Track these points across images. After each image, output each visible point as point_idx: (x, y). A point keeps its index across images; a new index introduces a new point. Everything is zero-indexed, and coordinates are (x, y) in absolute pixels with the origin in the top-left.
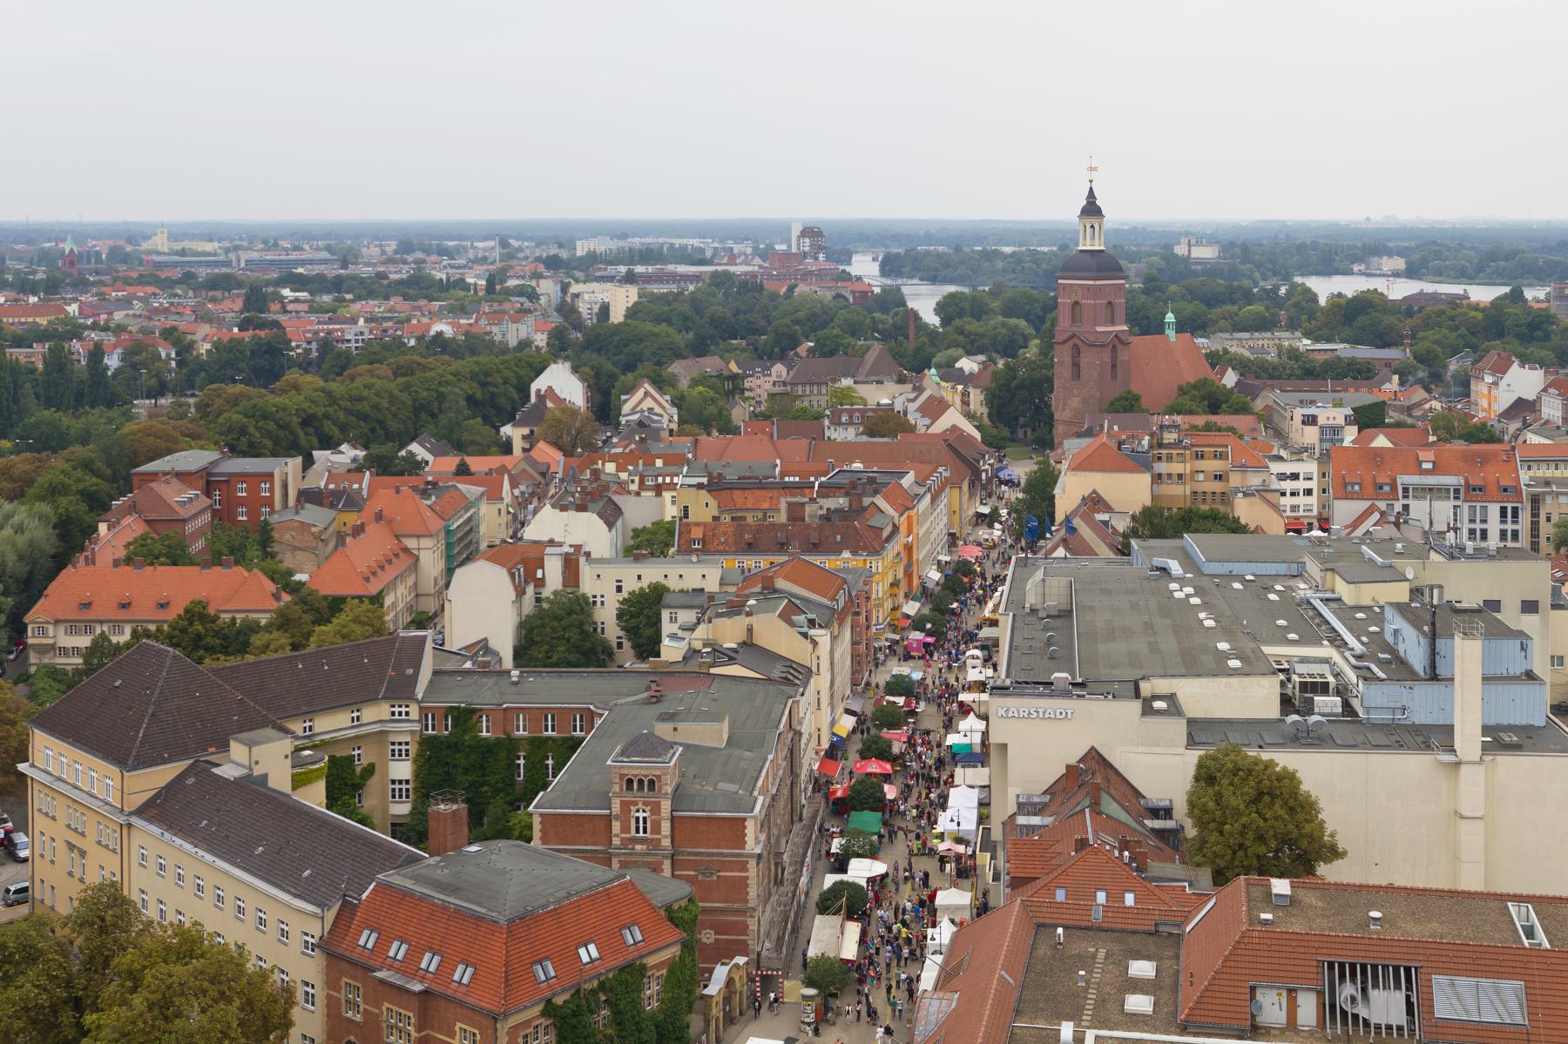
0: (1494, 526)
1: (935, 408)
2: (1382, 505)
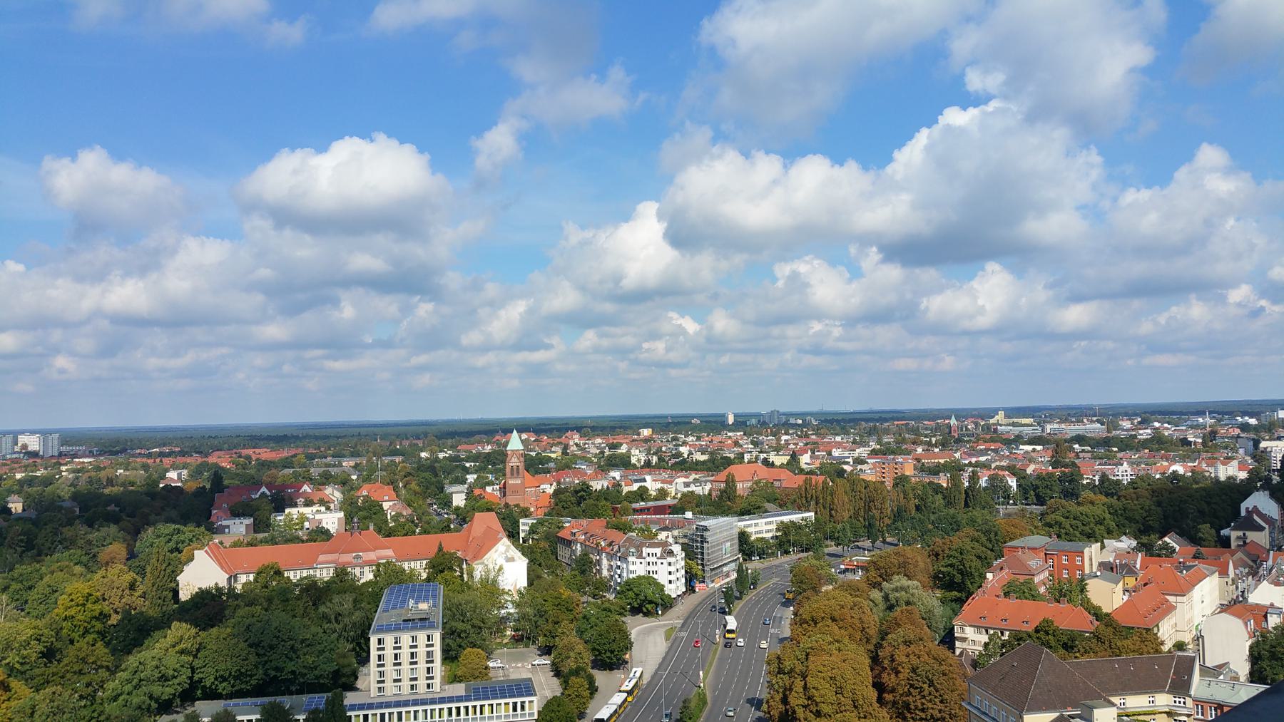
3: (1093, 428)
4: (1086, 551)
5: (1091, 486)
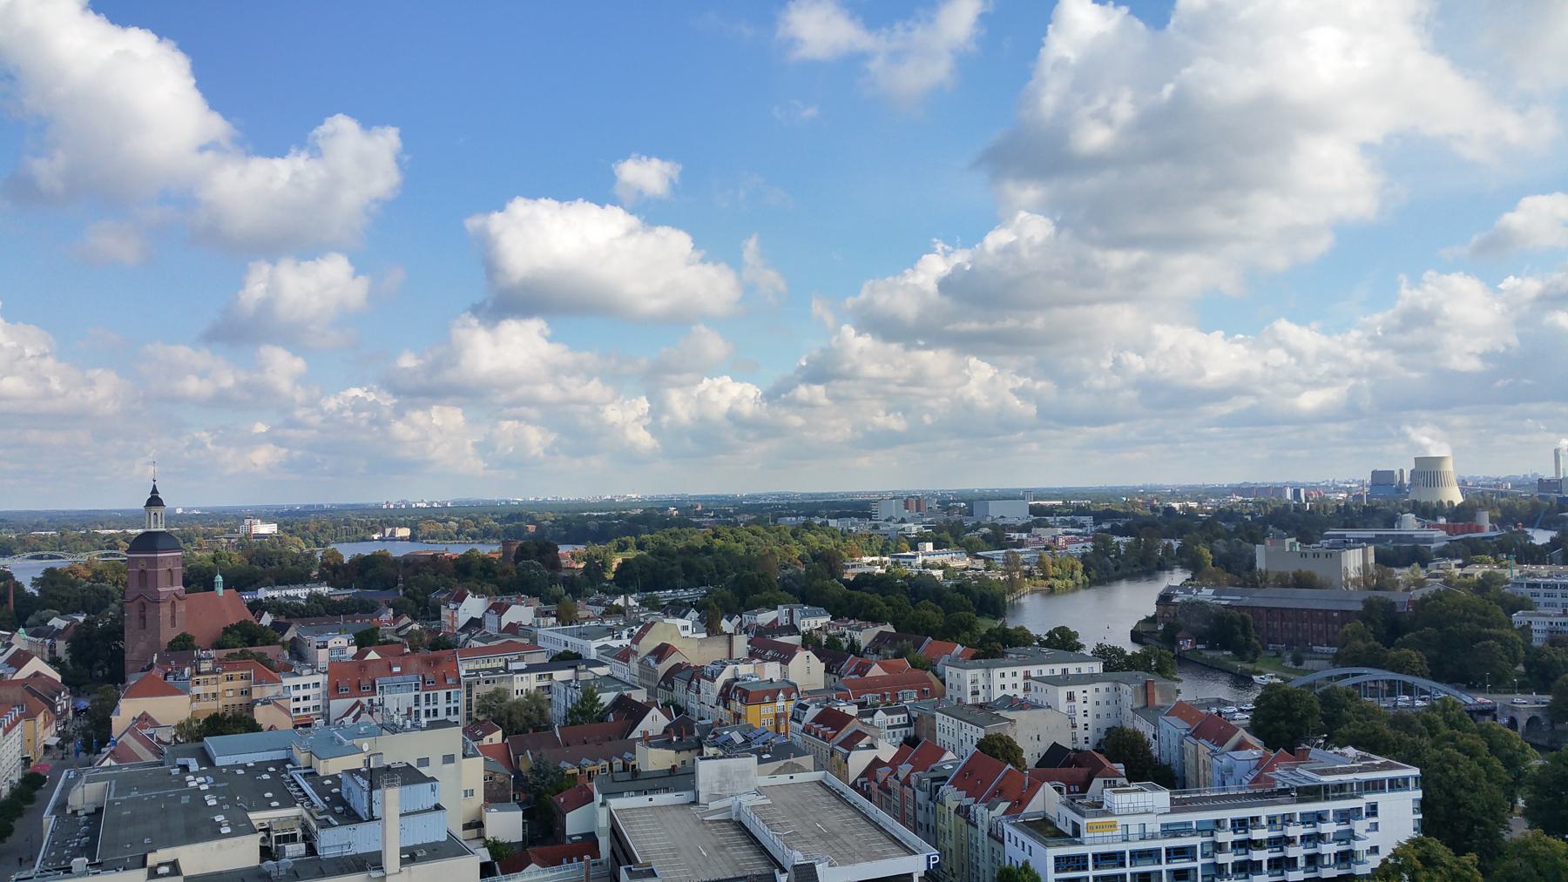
0: (442, 706)
1: (19, 660)
2: (364, 700)
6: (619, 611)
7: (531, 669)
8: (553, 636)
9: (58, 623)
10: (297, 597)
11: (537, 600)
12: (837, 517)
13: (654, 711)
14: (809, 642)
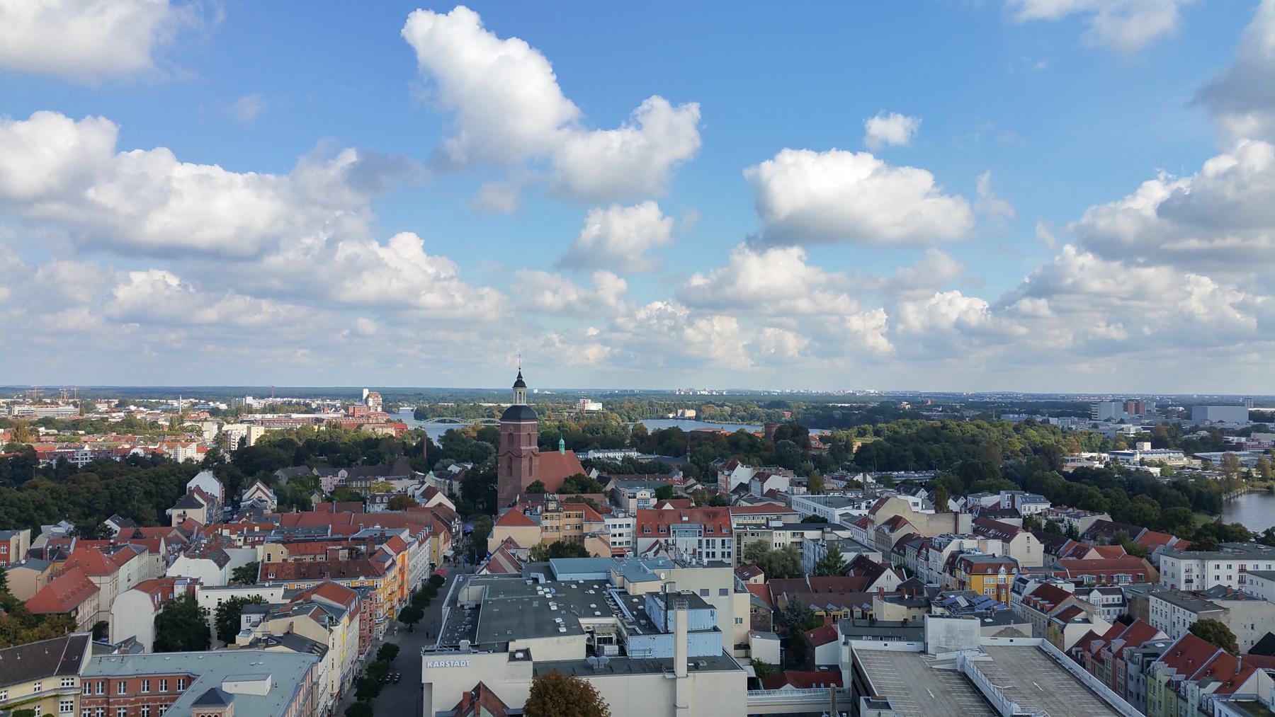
0: (718, 550)
1: (429, 493)
2: (662, 540)
3: (66, 411)
4: (13, 540)
5: (47, 471)
6: (859, 486)
7: (786, 527)
8: (805, 503)
9: (454, 468)
10: (615, 459)
11: (791, 472)
12: (1057, 415)
13: (888, 572)
14: (1030, 524)
